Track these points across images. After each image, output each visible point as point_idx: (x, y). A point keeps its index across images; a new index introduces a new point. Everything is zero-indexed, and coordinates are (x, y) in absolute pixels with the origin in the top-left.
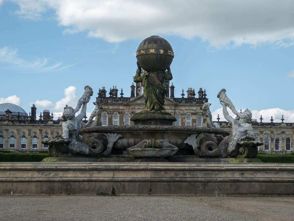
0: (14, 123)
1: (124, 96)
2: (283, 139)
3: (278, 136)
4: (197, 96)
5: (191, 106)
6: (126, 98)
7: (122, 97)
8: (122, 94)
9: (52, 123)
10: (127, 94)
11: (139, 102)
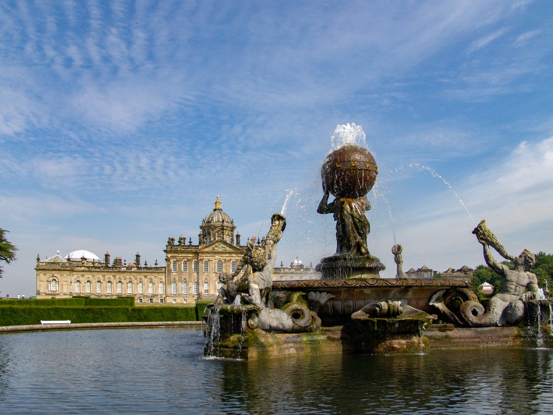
0: (89, 269)
6: (195, 246)
9: (125, 269)
10: (196, 242)
11: (207, 250)
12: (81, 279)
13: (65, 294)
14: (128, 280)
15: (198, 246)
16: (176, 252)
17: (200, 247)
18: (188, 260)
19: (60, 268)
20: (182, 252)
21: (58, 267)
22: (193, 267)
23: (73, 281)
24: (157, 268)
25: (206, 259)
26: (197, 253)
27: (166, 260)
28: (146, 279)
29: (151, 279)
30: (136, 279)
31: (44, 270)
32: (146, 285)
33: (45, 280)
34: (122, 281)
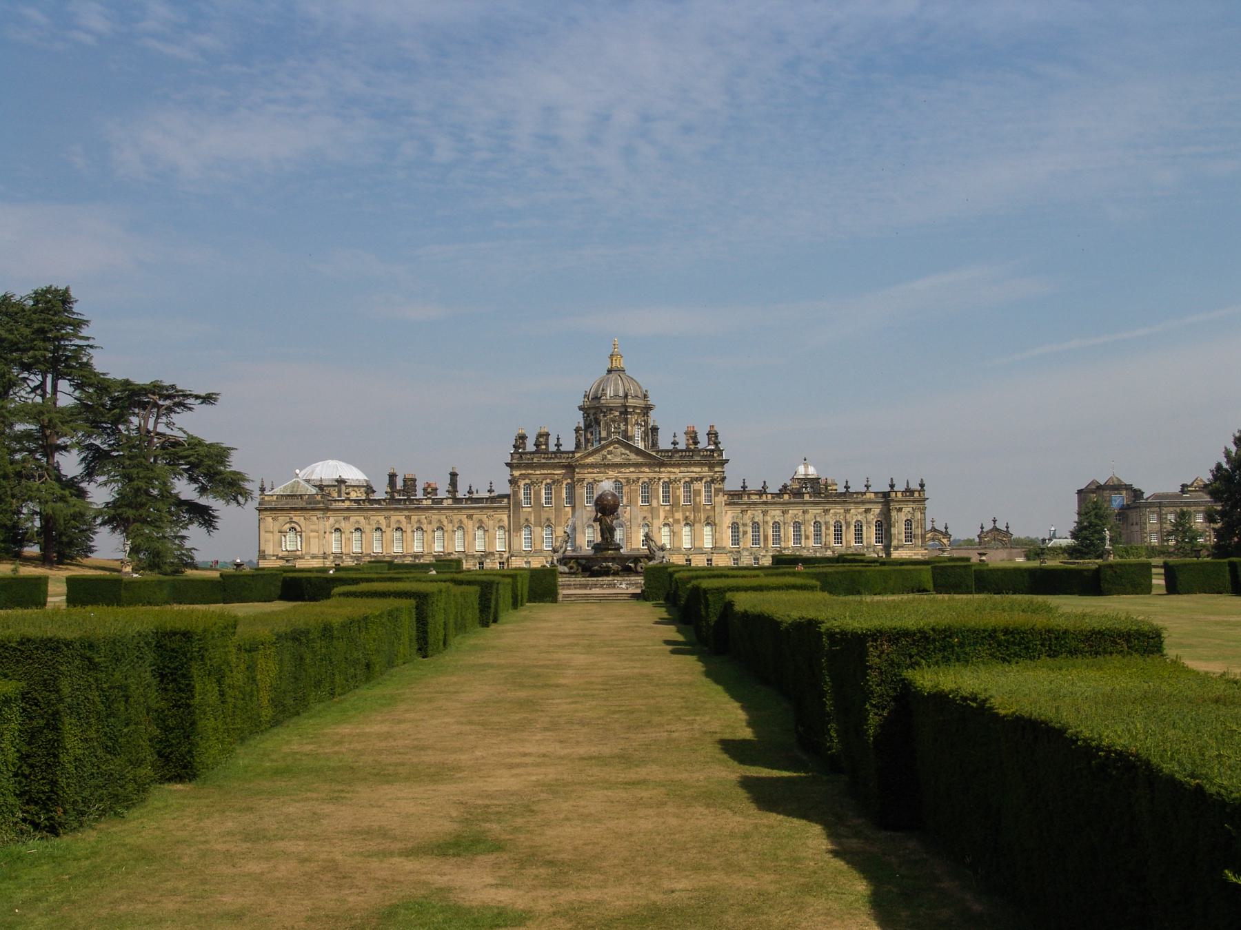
1: (562, 449)
2: (868, 523)
3: (859, 518)
4: (703, 443)
5: (691, 465)
7: (559, 451)
8: (558, 445)
9: (430, 502)
10: (569, 444)
11: (590, 460)
12: (343, 525)
13: (314, 557)
14: (435, 525)
15: (573, 452)
16: (528, 466)
17: (577, 455)
18: (554, 482)
19: (304, 505)
20: (542, 466)
21: (300, 504)
22: (564, 496)
23: (328, 530)
24: (492, 500)
25: (589, 478)
26: (571, 468)
27: (510, 481)
28: (471, 522)
29: (481, 521)
30: (451, 522)
31: (271, 509)
32: (471, 533)
33: (276, 529)
34: (424, 527)
